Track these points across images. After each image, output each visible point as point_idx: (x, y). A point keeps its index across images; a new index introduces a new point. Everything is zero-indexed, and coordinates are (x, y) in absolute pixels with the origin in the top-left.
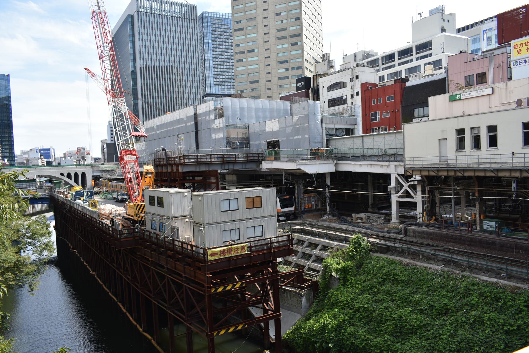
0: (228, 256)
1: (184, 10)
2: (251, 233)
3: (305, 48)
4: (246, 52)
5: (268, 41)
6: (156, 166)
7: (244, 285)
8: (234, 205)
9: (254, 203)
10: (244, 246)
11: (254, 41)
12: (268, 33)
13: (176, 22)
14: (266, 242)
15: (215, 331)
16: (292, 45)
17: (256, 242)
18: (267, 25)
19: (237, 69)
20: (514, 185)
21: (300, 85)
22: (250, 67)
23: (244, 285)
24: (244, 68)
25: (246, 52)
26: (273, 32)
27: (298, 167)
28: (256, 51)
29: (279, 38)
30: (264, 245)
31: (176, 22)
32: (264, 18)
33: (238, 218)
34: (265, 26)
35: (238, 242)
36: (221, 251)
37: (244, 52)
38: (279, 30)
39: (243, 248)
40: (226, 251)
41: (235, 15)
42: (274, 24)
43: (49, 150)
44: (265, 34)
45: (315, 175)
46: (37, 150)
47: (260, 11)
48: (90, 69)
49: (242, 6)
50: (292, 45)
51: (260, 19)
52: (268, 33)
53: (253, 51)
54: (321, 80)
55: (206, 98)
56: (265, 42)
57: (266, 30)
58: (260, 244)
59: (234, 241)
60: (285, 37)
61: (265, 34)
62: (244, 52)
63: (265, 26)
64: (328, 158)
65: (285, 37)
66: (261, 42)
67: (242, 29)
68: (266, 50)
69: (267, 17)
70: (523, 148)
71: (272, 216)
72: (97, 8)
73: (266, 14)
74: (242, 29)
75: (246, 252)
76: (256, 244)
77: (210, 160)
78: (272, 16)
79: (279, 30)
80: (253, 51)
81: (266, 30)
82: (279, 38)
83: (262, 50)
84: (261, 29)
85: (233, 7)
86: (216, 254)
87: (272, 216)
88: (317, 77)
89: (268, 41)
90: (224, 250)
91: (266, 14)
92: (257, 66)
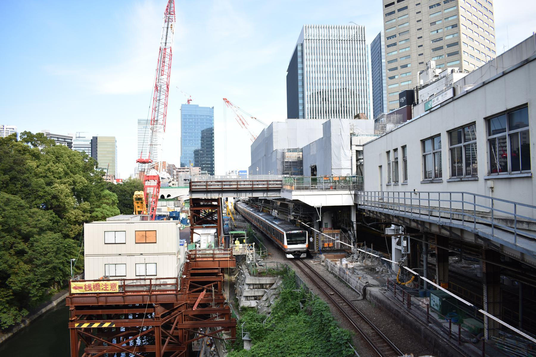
0: (93, 292)
1: (353, 32)
2: (141, 271)
3: (464, 56)
4: (399, 68)
5: (422, 54)
6: (192, 192)
7: (114, 326)
8: (120, 238)
9: (145, 238)
10: (115, 285)
11: (408, 57)
12: (422, 46)
13: (341, 45)
14: (148, 282)
16: (449, 55)
17: (135, 281)
18: (421, 37)
19: (390, 87)
21: (403, 100)
23: (114, 326)
24: (397, 85)
25: (399, 68)
26: (428, 44)
27: (294, 198)
28: (409, 66)
29: (435, 50)
30: (145, 285)
31: (341, 45)
32: (418, 30)
34: (418, 38)
35: (111, 278)
36: (85, 286)
37: (396, 69)
38: (434, 41)
39: (113, 286)
40: (92, 287)
41: (387, 31)
42: (428, 34)
44: (419, 46)
45: (318, 208)
47: (413, 22)
48: (228, 99)
49: (394, 21)
50: (449, 55)
51: (413, 31)
52: (422, 46)
53: (406, 66)
56: (419, 55)
57: (420, 42)
58: (138, 283)
59: (107, 276)
60: (441, 48)
61: (419, 46)
62: (396, 69)
63: (418, 38)
64: (343, 188)
65: (441, 48)
66: (414, 56)
67: (395, 44)
68: (420, 63)
69: (421, 29)
70: (423, 183)
71: (170, 254)
72: (164, 44)
73: (419, 25)
74: (395, 44)
76: (134, 284)
77: (235, 187)
78: (425, 25)
79: (434, 41)
80: (406, 66)
81: (420, 42)
82: (435, 50)
83: (415, 64)
84: (415, 42)
85: (385, 22)
86: (81, 288)
87: (170, 254)
89: (422, 54)
90: (89, 286)
91: (419, 25)
92: (410, 82)
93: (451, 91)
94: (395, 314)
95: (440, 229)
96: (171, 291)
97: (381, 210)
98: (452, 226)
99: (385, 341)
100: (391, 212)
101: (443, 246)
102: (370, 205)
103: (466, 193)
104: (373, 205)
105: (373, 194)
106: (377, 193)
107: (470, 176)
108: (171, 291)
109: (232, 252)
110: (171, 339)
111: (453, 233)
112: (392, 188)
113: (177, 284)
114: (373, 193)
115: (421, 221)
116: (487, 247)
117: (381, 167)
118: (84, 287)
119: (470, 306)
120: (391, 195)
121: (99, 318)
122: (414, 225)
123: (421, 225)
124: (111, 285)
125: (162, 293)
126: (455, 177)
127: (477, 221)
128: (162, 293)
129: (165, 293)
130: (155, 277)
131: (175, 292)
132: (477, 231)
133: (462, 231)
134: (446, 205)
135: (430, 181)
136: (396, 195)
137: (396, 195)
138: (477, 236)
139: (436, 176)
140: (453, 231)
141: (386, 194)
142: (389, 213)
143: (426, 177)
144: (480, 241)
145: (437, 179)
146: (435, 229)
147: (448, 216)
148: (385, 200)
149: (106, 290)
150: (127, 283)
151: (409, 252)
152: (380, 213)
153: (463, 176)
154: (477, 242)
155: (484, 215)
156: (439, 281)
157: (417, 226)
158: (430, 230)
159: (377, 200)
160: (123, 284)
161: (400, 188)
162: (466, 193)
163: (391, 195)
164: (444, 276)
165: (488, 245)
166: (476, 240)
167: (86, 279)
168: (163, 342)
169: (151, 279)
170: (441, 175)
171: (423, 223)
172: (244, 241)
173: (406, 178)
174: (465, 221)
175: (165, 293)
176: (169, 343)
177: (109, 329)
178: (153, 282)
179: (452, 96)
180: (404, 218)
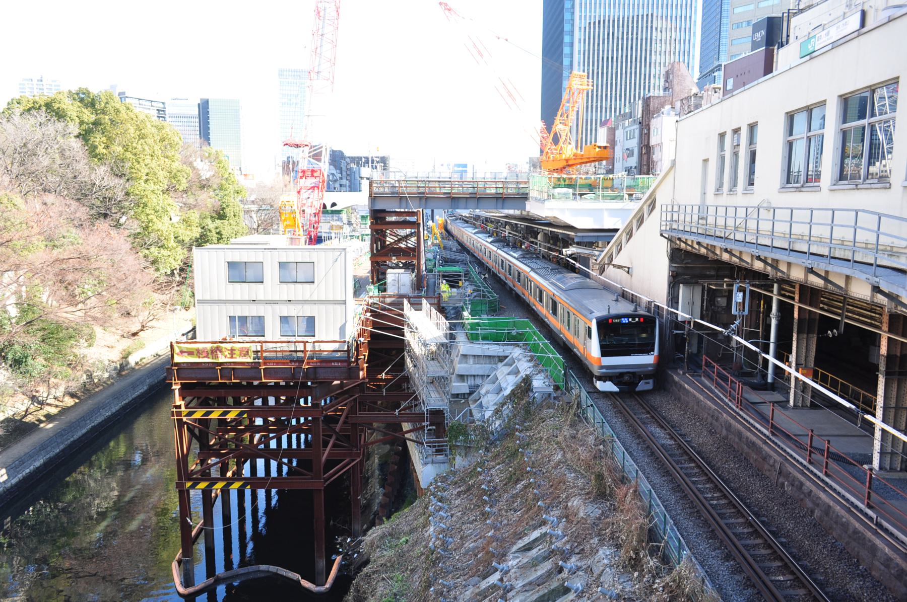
14: (300, 347)
15: (190, 480)
17: (279, 345)
19: (737, 11)
20: (738, 297)
22: (762, 5)
23: (245, 416)
24: (751, 7)
30: (296, 351)
33: (261, 297)
36: (198, 350)
43: (465, 166)
46: (449, 165)
54: (794, 21)
55: (716, 74)
75: (252, 361)
76: (278, 349)
88: (790, 14)
93: (858, 16)
94: (713, 416)
95: (806, 276)
96: (338, 361)
97: (701, 240)
98: (830, 268)
99: (691, 460)
100: (719, 244)
101: (810, 305)
102: (681, 228)
103: (863, 211)
104: (687, 229)
105: (689, 209)
106: (696, 209)
107: (876, 181)
108: (338, 361)
109: (439, 301)
110: (337, 439)
111: (831, 282)
112: (725, 199)
113: (348, 351)
114: (689, 209)
115: (773, 260)
116: (894, 310)
117: (706, 161)
118: (195, 353)
119: (849, 409)
120: (721, 211)
121: (222, 403)
122: (758, 265)
123: (771, 266)
124: (241, 350)
125: (324, 365)
126: (846, 182)
127: (879, 263)
128: (324, 365)
129: (329, 365)
130: (313, 339)
131: (345, 364)
132: (877, 280)
133: (848, 278)
134: (824, 232)
135: (797, 188)
136: (731, 211)
137: (731, 211)
138: (876, 289)
139: (807, 180)
140: (830, 278)
141: (712, 210)
142: (715, 243)
143: (788, 182)
144: (881, 299)
145: (811, 184)
146: (797, 274)
147: (825, 252)
148: (711, 220)
149: (232, 357)
150: (266, 346)
151: (746, 312)
152: (699, 243)
153: (861, 181)
154: (875, 300)
155: (892, 252)
156: (797, 364)
157: (765, 268)
158: (788, 276)
159: (695, 218)
160: (259, 349)
161: (740, 199)
162: (863, 211)
163: (721, 211)
164: (806, 357)
165: (896, 307)
166: (872, 296)
167: (197, 340)
168: (325, 444)
169: (305, 343)
170: (818, 177)
171: (775, 264)
172: (460, 284)
173: (751, 183)
174: (856, 262)
175: (329, 365)
176: (334, 445)
177: (238, 421)
178: (309, 347)
179: (857, 25)
180: (741, 252)
